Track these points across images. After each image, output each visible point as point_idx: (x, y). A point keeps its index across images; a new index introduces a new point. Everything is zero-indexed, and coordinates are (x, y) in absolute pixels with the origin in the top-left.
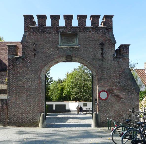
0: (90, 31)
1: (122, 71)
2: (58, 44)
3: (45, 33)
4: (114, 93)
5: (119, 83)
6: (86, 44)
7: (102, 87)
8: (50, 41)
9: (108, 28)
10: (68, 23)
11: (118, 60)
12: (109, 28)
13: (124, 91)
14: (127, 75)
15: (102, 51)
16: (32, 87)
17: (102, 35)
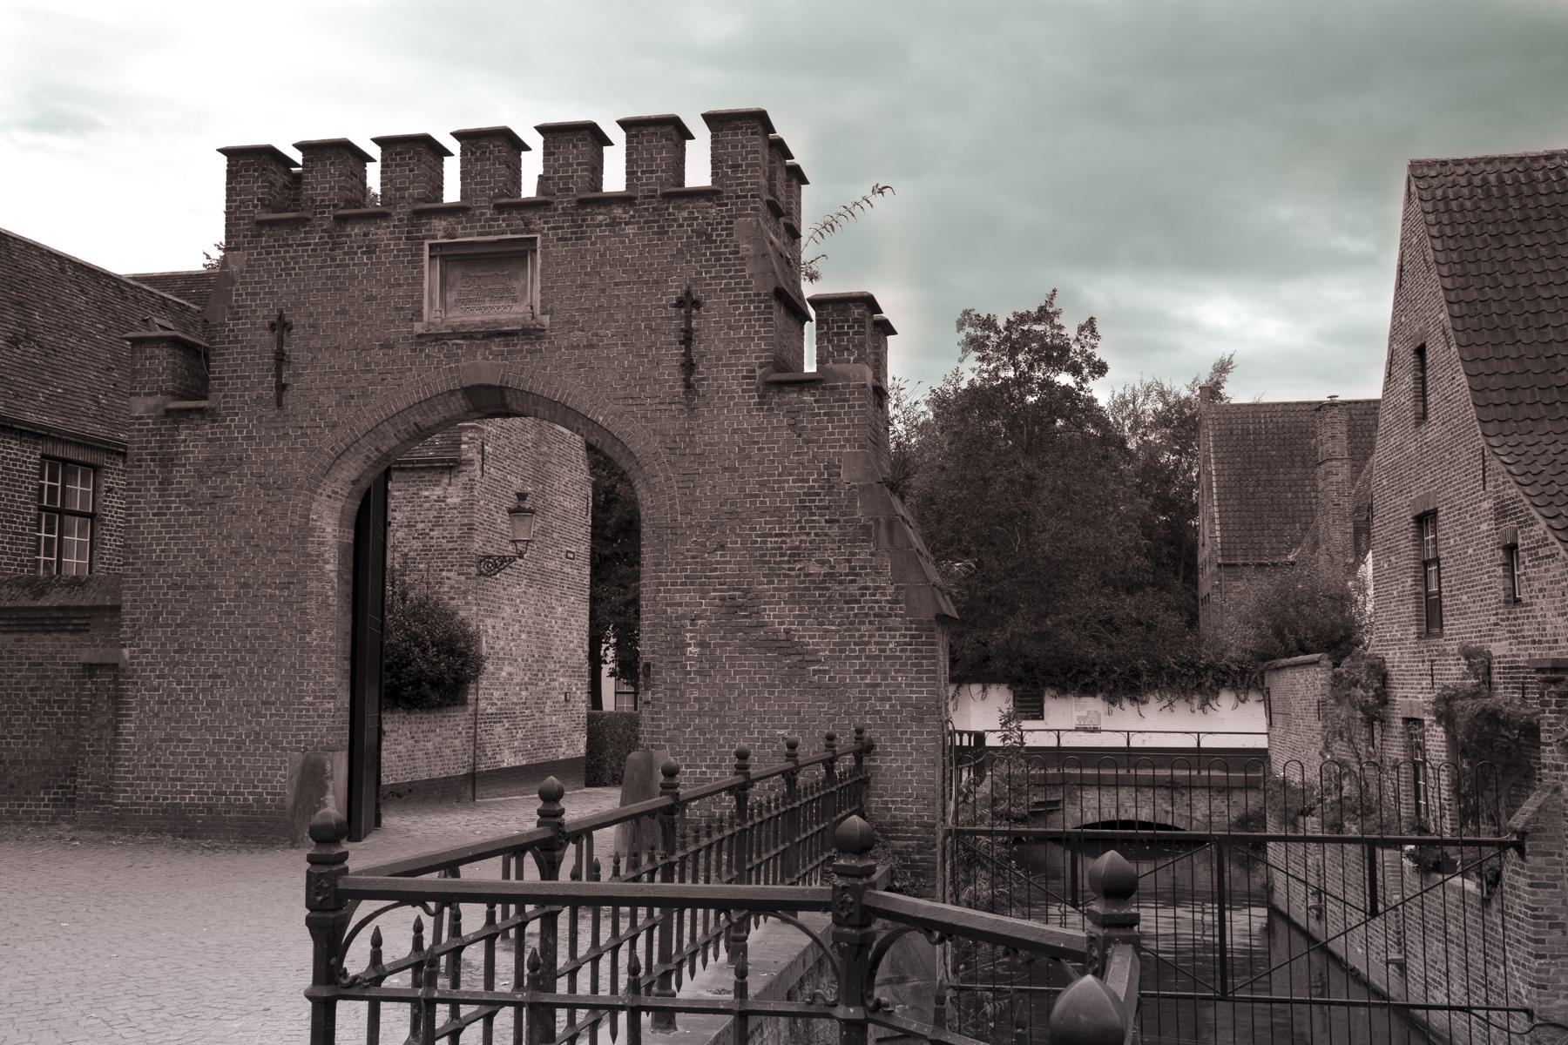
0: (614, 223)
1: (821, 474)
2: (418, 315)
3: (345, 254)
5: (796, 555)
6: (589, 310)
8: (371, 298)
9: (728, 198)
10: (476, 184)
11: (789, 403)
13: (831, 609)
14: (852, 500)
15: (688, 348)
17: (689, 245)
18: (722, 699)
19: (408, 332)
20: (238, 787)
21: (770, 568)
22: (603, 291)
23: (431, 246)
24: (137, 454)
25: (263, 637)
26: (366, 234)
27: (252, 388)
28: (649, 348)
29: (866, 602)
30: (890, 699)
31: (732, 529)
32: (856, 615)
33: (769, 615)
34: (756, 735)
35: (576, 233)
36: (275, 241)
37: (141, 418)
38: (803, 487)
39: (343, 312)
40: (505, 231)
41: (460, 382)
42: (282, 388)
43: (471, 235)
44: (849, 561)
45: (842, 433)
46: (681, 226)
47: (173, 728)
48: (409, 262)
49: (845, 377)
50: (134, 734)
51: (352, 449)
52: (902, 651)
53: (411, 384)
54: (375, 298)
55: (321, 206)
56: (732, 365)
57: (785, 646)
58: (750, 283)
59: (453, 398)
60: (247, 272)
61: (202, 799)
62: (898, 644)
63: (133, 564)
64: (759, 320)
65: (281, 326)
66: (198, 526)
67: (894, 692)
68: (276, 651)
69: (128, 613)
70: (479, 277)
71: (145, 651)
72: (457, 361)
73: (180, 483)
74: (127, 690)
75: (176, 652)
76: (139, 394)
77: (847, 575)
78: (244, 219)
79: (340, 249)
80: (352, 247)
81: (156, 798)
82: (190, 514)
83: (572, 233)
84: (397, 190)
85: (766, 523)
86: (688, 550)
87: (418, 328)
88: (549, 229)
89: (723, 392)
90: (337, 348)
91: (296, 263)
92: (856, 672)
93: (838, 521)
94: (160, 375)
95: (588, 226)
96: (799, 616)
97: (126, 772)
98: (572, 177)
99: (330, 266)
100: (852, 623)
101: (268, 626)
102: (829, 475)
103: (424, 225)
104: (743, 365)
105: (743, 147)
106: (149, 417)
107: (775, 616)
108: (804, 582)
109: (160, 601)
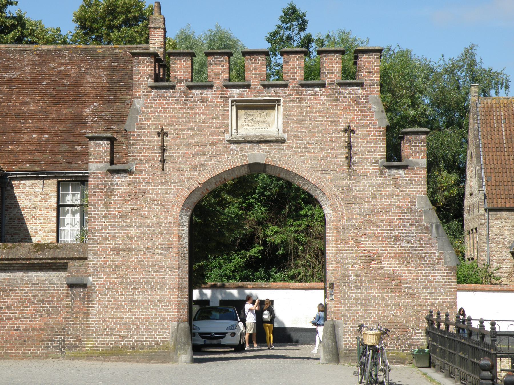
2: (226, 131)
3: (192, 102)
4: (382, 268)
5: (397, 238)
6: (305, 132)
7: (348, 250)
8: (204, 123)
9: (366, 86)
10: (253, 74)
11: (394, 175)
12: (371, 86)
13: (412, 261)
16: (157, 251)
18: (366, 299)
19: (223, 139)
20: (147, 338)
21: (386, 244)
22: (311, 124)
23: (233, 101)
24: (93, 189)
25: (157, 272)
26: (201, 94)
27: (149, 161)
28: (332, 150)
29: (427, 258)
30: (438, 299)
31: (369, 227)
32: (423, 264)
33: (385, 263)
34: (381, 314)
35: (299, 98)
36: (158, 95)
37: (95, 173)
38: (400, 210)
39: (191, 128)
40: (267, 95)
41: (247, 162)
42: (163, 161)
43: (251, 97)
44: (420, 241)
45: (416, 188)
46: (345, 97)
47: (115, 312)
48: (222, 107)
49: (417, 164)
50: (95, 315)
51: (197, 189)
52: (443, 279)
53: (225, 162)
54: (207, 123)
55: (179, 80)
56: (368, 158)
57: (393, 276)
58: (376, 123)
59: (243, 168)
60: (145, 108)
61: (130, 344)
62: (441, 276)
63: (93, 239)
64: (380, 139)
65: (163, 133)
66: (125, 222)
67: (440, 296)
68: (164, 278)
69: (91, 261)
70: (253, 115)
71: (100, 278)
72: (245, 152)
73: (115, 203)
74: (92, 296)
75: (115, 278)
76: (93, 162)
77: (419, 247)
78: (142, 84)
79: (190, 100)
80: (195, 100)
81: (107, 344)
82: (120, 217)
83: (297, 98)
84: (217, 75)
85: (384, 225)
86: (350, 236)
87: (228, 137)
88: (286, 96)
89: (365, 169)
90: (189, 144)
91: (169, 105)
92: (424, 288)
93: (415, 225)
94: (103, 153)
95: (304, 95)
96: (398, 264)
97: (92, 332)
98: (296, 73)
99: (185, 108)
100: (421, 267)
101: (159, 266)
102: (411, 205)
103: (228, 91)
104: (373, 158)
105: (373, 63)
106: (99, 173)
107: (388, 264)
108: (400, 250)
109: (107, 255)
